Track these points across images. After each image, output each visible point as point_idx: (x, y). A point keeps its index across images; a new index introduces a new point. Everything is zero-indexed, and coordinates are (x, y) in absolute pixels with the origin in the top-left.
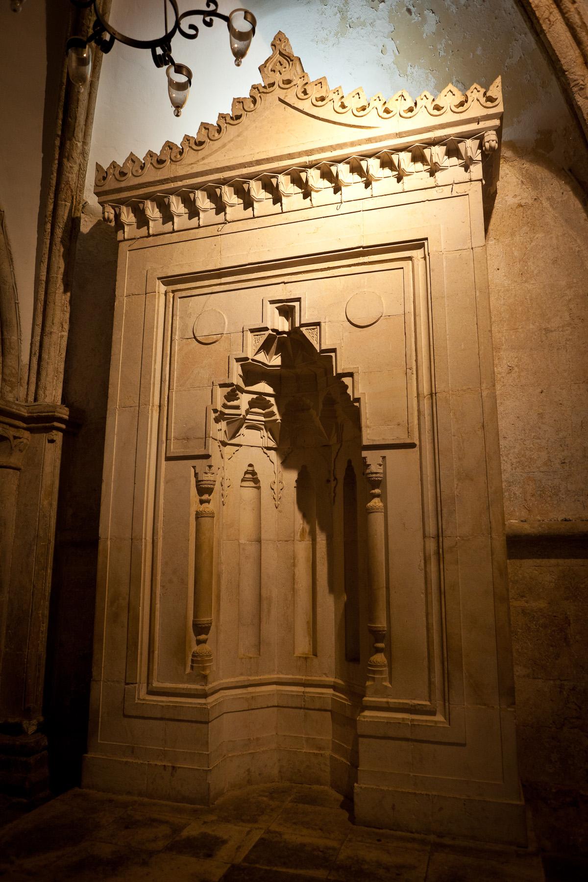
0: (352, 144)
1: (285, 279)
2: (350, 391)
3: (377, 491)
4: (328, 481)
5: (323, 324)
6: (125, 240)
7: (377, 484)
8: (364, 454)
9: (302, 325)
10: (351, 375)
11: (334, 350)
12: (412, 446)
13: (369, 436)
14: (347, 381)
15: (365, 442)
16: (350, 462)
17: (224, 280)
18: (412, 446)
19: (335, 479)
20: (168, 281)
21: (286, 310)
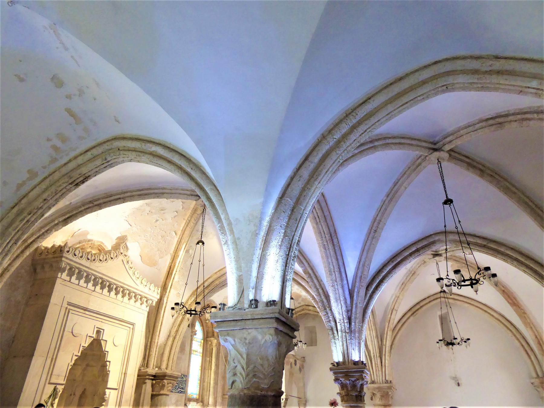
0: (133, 288)
1: (103, 321)
2: (108, 367)
3: (104, 404)
4: (71, 395)
5: (108, 342)
6: (61, 278)
7: (104, 400)
8: (107, 390)
9: (102, 340)
10: (110, 362)
11: (108, 352)
12: (116, 389)
13: (109, 386)
14: (108, 363)
15: (109, 386)
16: (85, 389)
17: (87, 313)
18: (116, 389)
19: (74, 394)
20: (69, 304)
21: (98, 332)
